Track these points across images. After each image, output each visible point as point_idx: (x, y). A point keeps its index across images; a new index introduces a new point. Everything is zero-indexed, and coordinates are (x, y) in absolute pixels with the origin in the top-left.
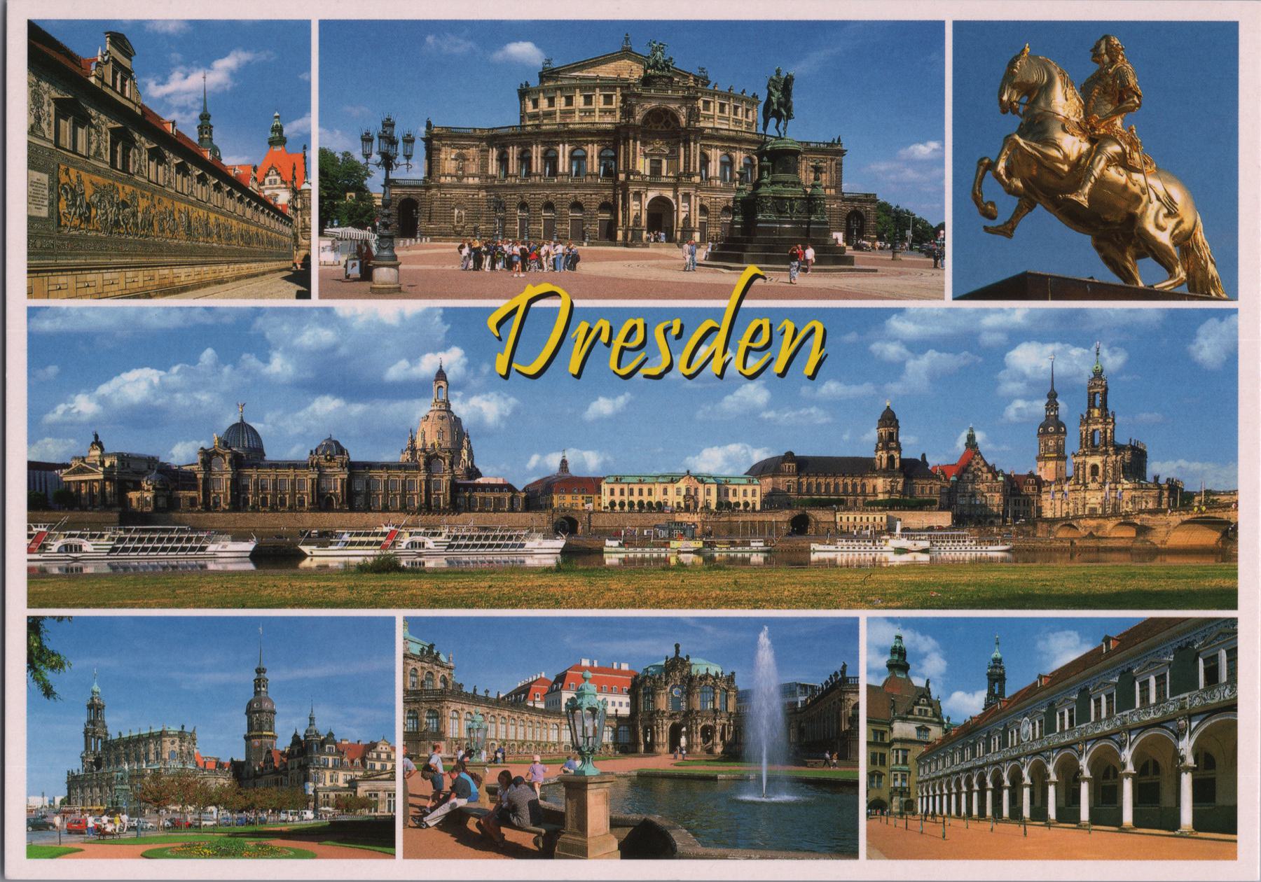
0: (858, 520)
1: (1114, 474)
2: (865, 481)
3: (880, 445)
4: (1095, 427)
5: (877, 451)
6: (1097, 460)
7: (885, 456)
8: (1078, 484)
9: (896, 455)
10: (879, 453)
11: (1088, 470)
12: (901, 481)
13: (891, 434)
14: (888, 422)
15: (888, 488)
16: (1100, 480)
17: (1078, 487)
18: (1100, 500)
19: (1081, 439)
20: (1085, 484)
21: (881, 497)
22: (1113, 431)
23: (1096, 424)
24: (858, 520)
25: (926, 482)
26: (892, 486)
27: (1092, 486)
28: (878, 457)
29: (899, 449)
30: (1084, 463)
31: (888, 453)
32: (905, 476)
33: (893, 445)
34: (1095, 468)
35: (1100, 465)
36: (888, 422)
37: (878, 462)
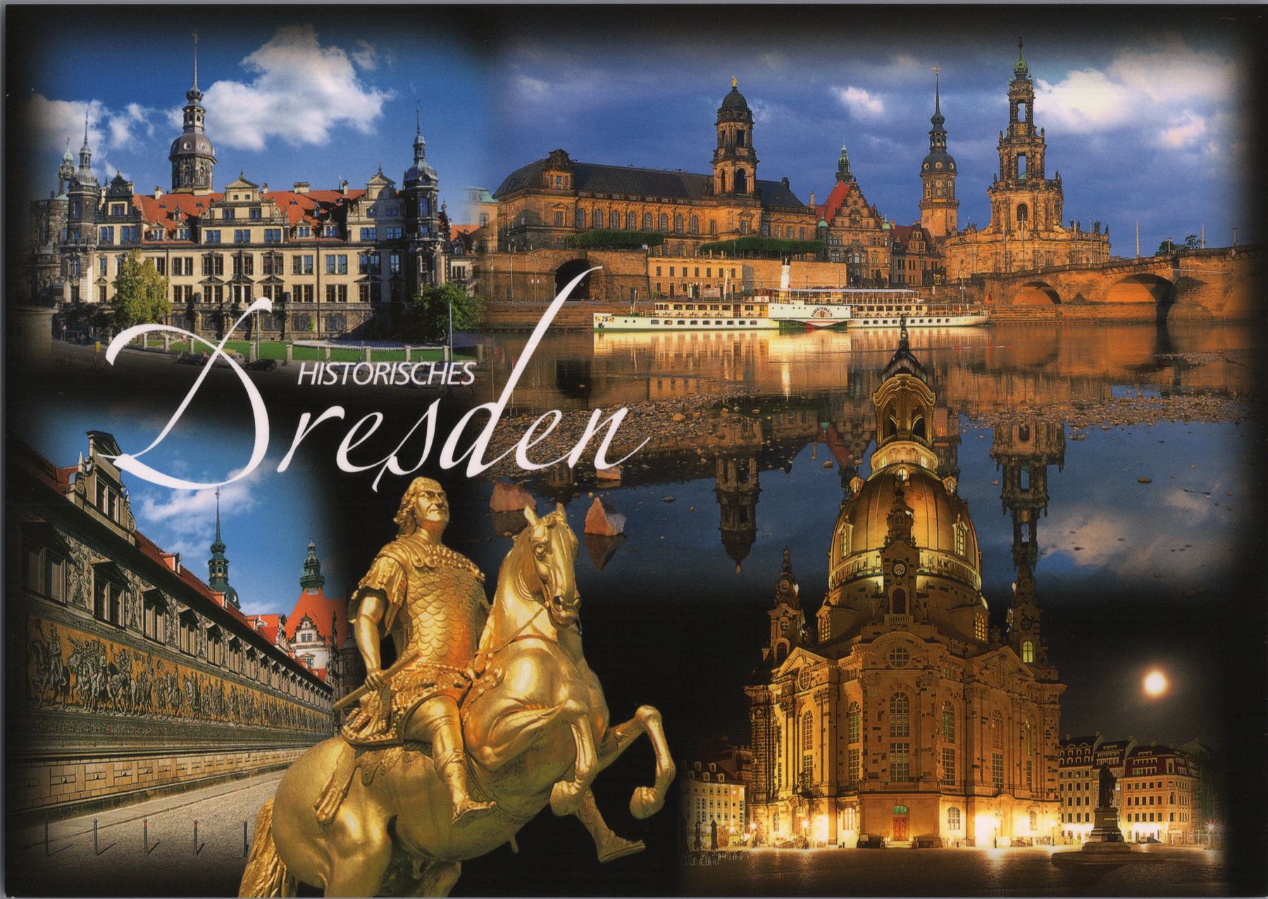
0: (691, 273)
1: (1047, 219)
2: (697, 212)
3: (722, 152)
4: (1021, 150)
5: (715, 162)
6: (1024, 197)
7: (730, 169)
8: (999, 231)
9: (749, 170)
10: (721, 165)
11: (1014, 212)
12: (757, 213)
13: (740, 134)
14: (735, 113)
15: (737, 225)
16: (1032, 227)
17: (999, 237)
18: (1030, 255)
19: (1002, 167)
20: (1010, 232)
21: (724, 238)
22: (1042, 157)
23: (1022, 145)
24: (691, 273)
25: (794, 218)
26: (742, 223)
27: (1018, 235)
28: (717, 172)
29: (754, 161)
30: (1007, 203)
31: (734, 164)
32: (762, 205)
33: (743, 152)
34: (1022, 208)
35: (1029, 205)
36: (735, 113)
37: (718, 182)
